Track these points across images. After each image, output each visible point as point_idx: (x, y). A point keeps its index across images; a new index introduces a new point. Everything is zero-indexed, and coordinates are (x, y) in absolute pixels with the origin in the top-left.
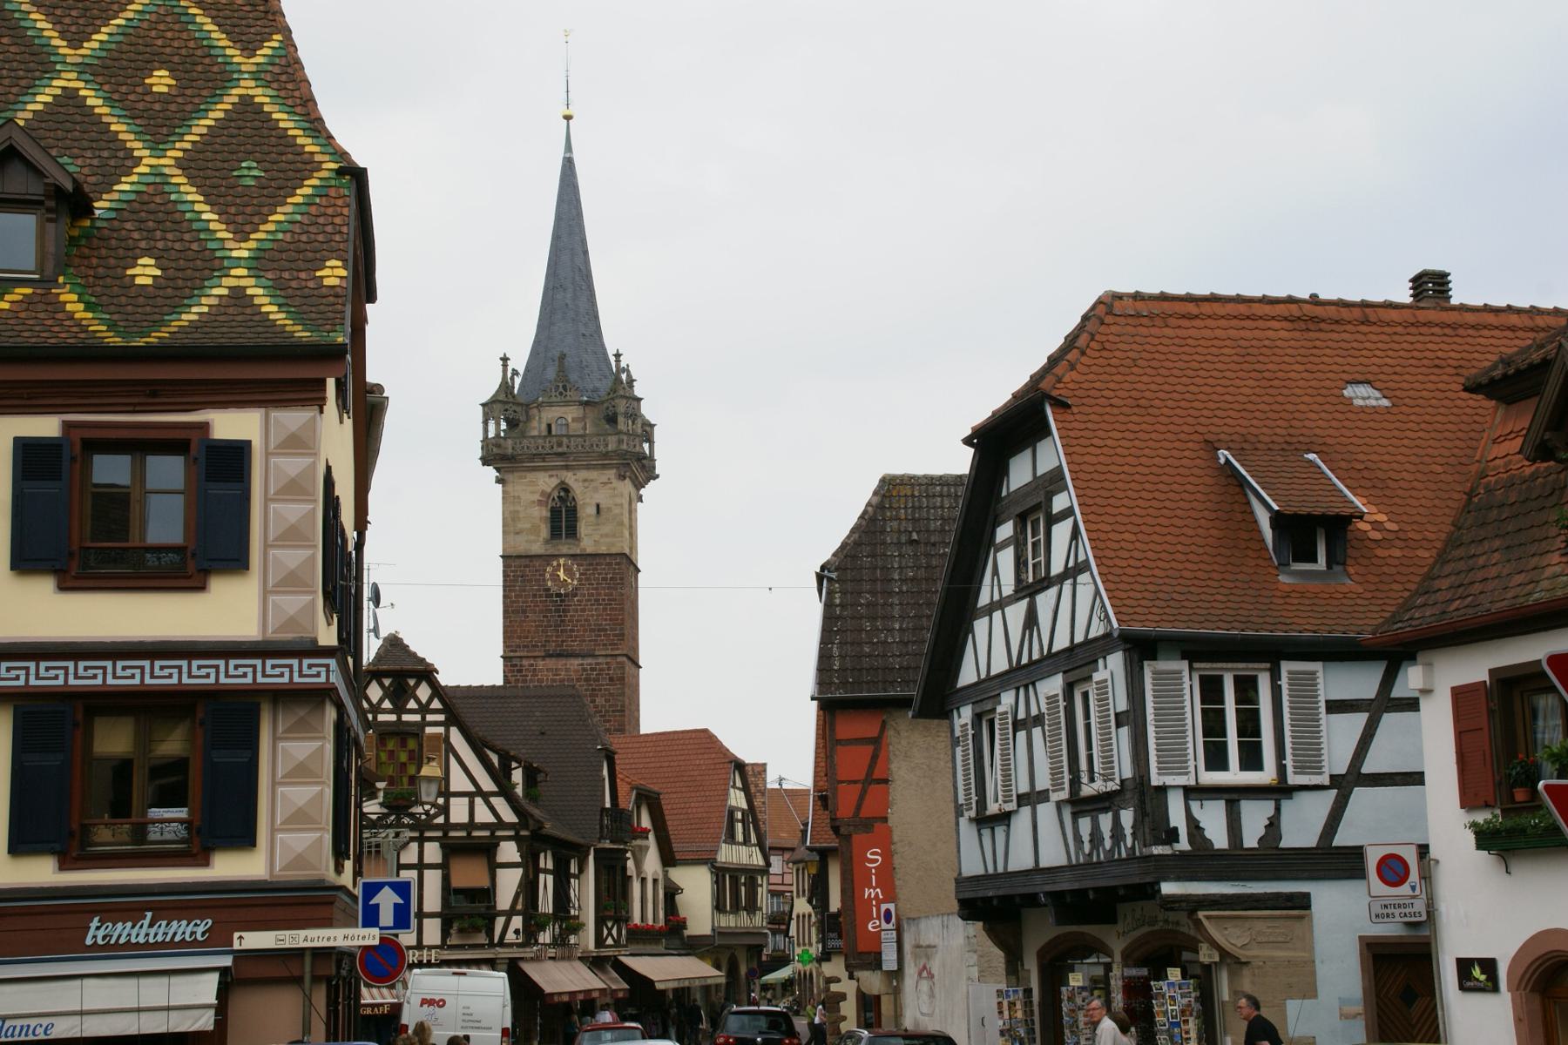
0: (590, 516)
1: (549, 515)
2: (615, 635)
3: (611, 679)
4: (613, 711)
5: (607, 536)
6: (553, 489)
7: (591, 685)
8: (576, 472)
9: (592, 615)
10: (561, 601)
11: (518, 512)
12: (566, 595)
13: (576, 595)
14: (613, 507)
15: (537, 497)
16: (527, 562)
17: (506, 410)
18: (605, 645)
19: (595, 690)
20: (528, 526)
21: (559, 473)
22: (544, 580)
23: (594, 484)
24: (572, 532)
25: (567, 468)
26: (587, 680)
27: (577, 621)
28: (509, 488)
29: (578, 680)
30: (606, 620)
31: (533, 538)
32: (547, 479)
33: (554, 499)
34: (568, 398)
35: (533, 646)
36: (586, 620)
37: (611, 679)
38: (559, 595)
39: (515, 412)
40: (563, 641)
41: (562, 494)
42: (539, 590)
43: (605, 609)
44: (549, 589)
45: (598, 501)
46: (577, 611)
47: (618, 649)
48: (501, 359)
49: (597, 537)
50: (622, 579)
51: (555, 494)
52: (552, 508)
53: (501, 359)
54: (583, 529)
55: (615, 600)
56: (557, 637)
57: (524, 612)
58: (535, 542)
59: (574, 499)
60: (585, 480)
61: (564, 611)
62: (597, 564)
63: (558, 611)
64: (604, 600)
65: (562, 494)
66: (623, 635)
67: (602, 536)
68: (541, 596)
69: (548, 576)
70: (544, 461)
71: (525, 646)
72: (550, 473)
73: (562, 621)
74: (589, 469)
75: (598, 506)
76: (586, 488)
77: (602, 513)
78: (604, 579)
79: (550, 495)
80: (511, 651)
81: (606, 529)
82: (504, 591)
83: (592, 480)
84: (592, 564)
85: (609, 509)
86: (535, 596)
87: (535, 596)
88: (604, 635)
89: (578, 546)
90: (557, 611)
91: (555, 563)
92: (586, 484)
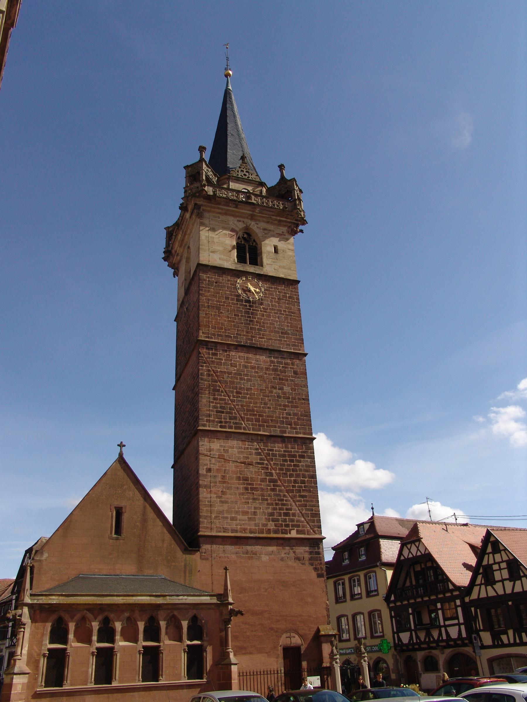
2: (296, 339)
3: (295, 373)
4: (299, 399)
5: (283, 267)
7: (278, 375)
8: (258, 222)
13: (262, 304)
14: (287, 250)
18: (289, 345)
19: (283, 380)
21: (246, 220)
22: (235, 288)
25: (252, 217)
26: (275, 370)
29: (267, 369)
31: (225, 258)
32: (236, 222)
34: (250, 178)
35: (226, 336)
36: (271, 324)
37: (295, 373)
40: (252, 337)
41: (245, 236)
43: (286, 318)
44: (239, 296)
46: (263, 315)
47: (299, 350)
49: (276, 267)
54: (266, 260)
56: (247, 332)
57: (219, 309)
58: (227, 261)
59: (254, 241)
60: (265, 229)
63: (248, 313)
65: (245, 236)
67: (280, 267)
68: (232, 299)
71: (218, 335)
72: (238, 219)
73: (251, 321)
76: (266, 234)
80: (206, 337)
83: (270, 230)
86: (227, 298)
87: (227, 298)
88: (287, 338)
89: (262, 270)
92: (266, 232)
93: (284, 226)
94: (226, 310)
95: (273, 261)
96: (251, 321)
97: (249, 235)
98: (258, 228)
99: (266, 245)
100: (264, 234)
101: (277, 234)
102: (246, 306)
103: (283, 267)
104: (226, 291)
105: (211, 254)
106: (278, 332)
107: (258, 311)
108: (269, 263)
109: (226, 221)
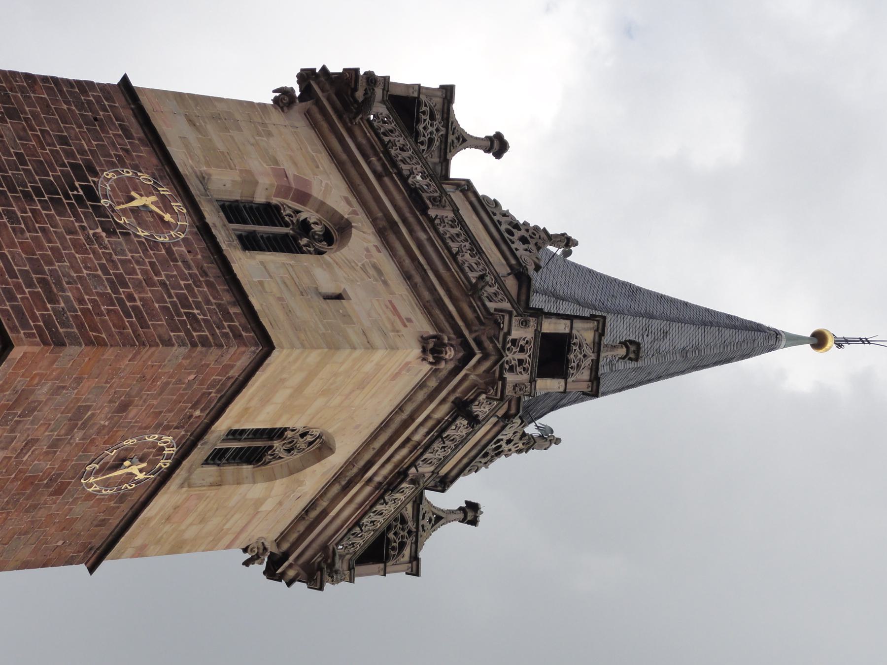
0: (308, 272)
1: (260, 198)
5: (288, 312)
6: (321, 207)
9: (78, 271)
10: (78, 198)
11: (239, 129)
12: (99, 211)
13: (111, 233)
15: (291, 172)
16: (137, 131)
17: (432, 117)
20: (220, 146)
22: (112, 165)
23: (380, 286)
24: (250, 243)
27: (43, 230)
28: (277, 117)
30: (81, 301)
33: (297, 212)
38: (91, 194)
39: (431, 141)
42: (82, 152)
45: (350, 293)
46: (71, 232)
48: (499, 136)
50: (204, 342)
51: (309, 214)
52: (277, 208)
53: (499, 136)
54: (275, 260)
55: (144, 325)
60: (379, 272)
61: (57, 203)
62: (210, 285)
64: (131, 298)
66: (60, 343)
69: (128, 173)
70: (379, 177)
72: (354, 201)
74: (407, 277)
75: (339, 297)
76: (363, 268)
77: (338, 292)
78: (183, 300)
79: (303, 197)
81: (303, 312)
82: (45, 79)
83: (385, 283)
84: (204, 273)
85: (347, 318)
87: (63, 141)
90: (51, 189)
91: (165, 191)
92: (372, 272)
93: (436, 324)
94: (22, 133)
95: (289, 282)
96: (27, 195)
97: (328, 238)
98: (367, 250)
99: (324, 266)
100: (360, 264)
101: (390, 302)
102: (74, 188)
103: (288, 312)
104: (89, 143)
105: (183, 120)
106: (39, 270)
107: (78, 219)
108: (271, 267)
109: (318, 167)
